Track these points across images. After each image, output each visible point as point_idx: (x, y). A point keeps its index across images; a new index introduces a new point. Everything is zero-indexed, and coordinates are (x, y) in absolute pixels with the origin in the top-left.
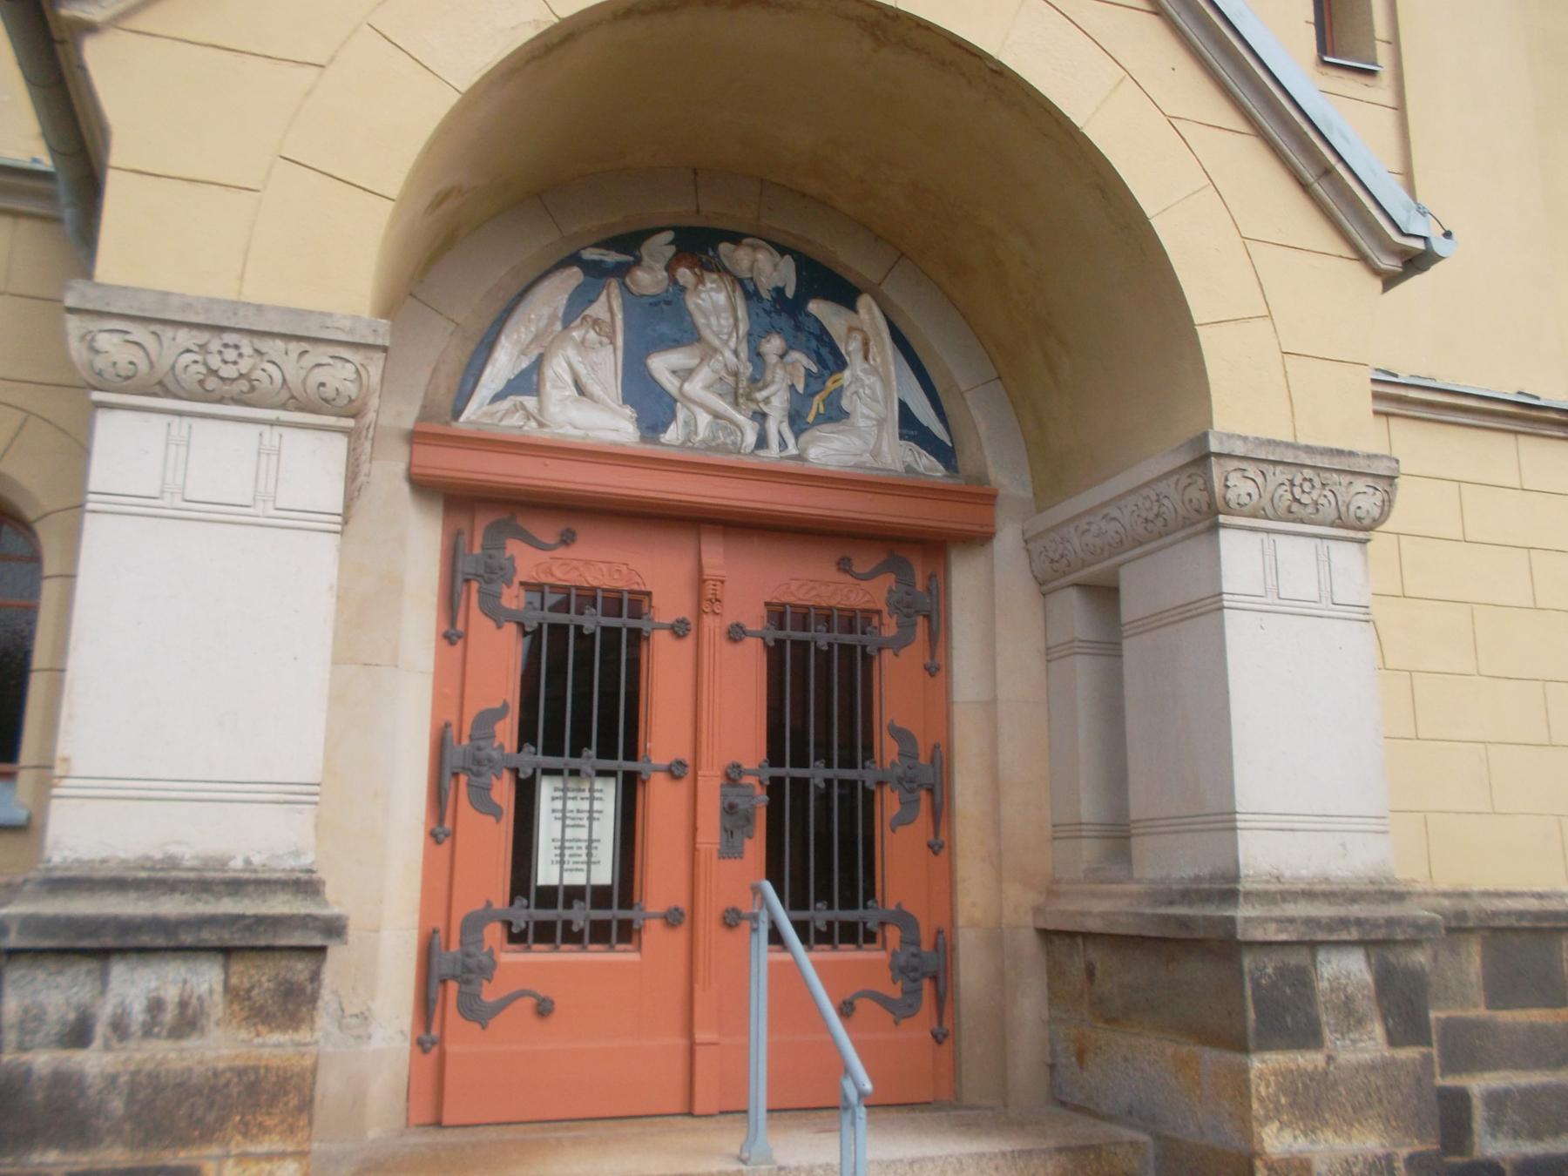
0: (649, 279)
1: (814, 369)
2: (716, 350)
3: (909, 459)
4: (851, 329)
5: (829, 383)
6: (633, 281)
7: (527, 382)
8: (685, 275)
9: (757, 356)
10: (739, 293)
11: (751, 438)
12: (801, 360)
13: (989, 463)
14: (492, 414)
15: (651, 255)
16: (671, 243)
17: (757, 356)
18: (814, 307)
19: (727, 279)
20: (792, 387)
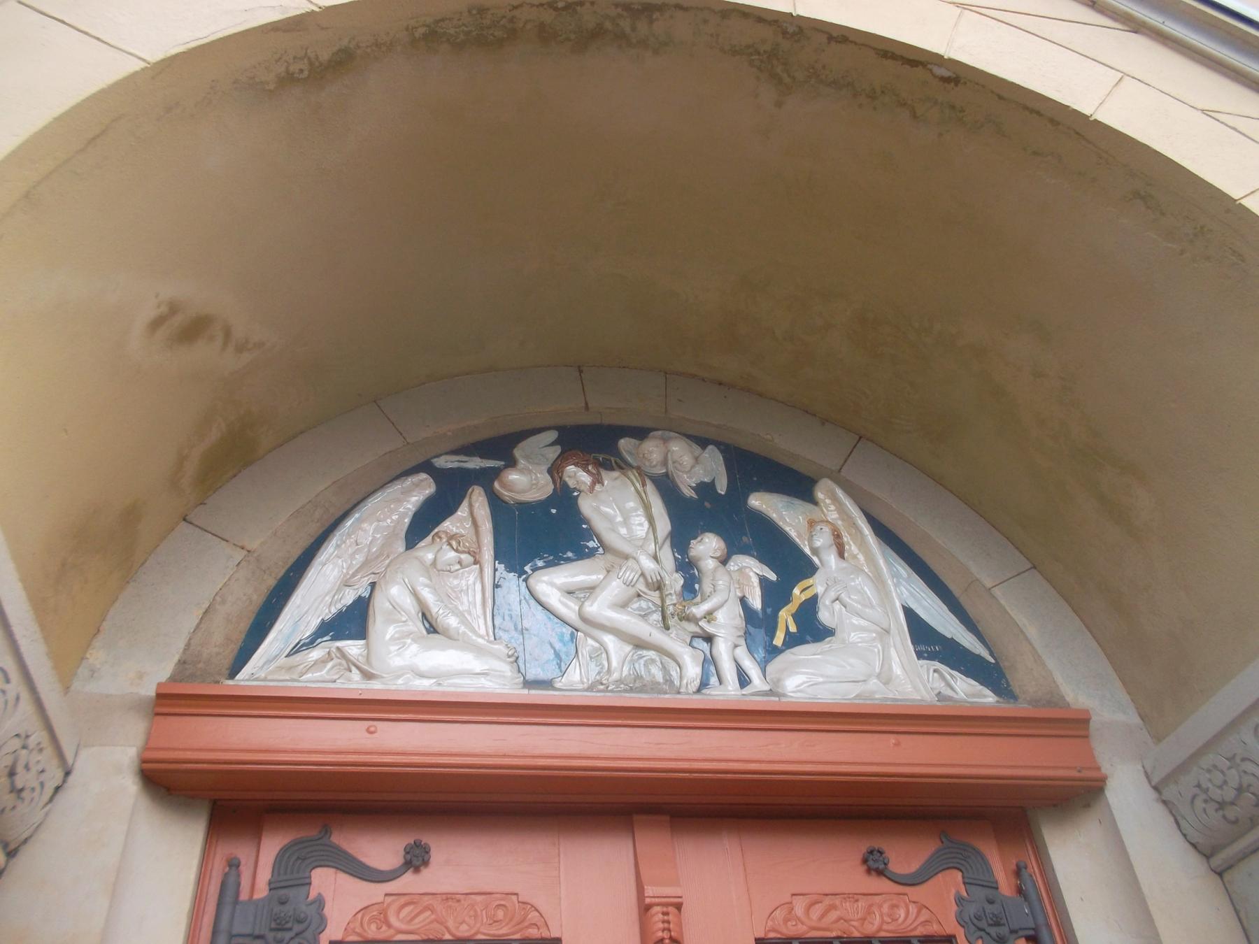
0: (526, 481)
1: (772, 576)
2: (626, 557)
3: (940, 685)
4: (812, 524)
5: (796, 591)
6: (504, 486)
7: (352, 621)
8: (577, 475)
9: (687, 566)
10: (650, 487)
11: (693, 671)
12: (751, 572)
13: (1059, 679)
14: (290, 669)
15: (527, 458)
16: (552, 444)
17: (687, 566)
18: (757, 501)
19: (633, 475)
20: (743, 601)
